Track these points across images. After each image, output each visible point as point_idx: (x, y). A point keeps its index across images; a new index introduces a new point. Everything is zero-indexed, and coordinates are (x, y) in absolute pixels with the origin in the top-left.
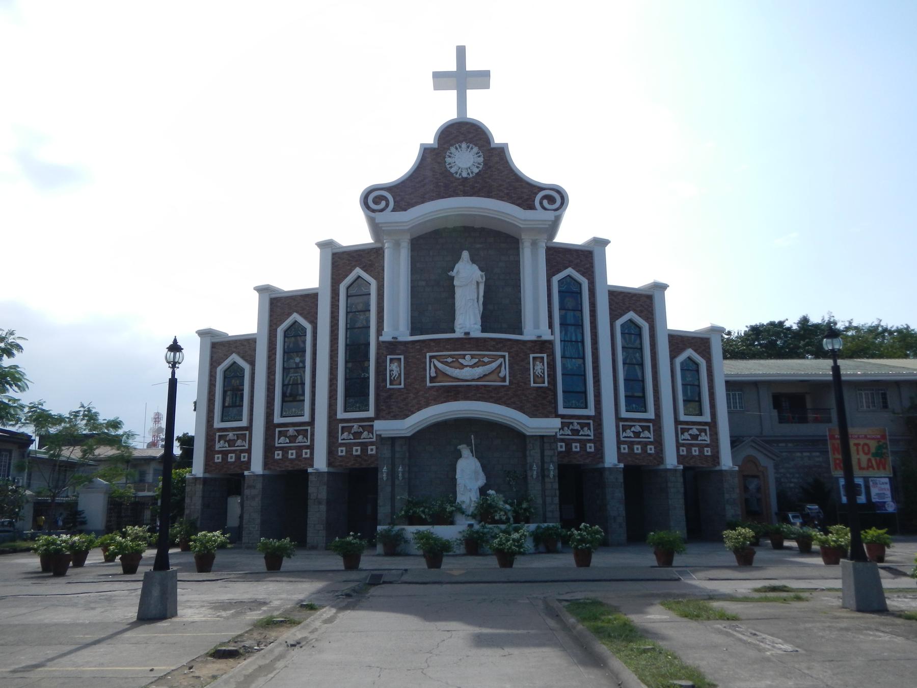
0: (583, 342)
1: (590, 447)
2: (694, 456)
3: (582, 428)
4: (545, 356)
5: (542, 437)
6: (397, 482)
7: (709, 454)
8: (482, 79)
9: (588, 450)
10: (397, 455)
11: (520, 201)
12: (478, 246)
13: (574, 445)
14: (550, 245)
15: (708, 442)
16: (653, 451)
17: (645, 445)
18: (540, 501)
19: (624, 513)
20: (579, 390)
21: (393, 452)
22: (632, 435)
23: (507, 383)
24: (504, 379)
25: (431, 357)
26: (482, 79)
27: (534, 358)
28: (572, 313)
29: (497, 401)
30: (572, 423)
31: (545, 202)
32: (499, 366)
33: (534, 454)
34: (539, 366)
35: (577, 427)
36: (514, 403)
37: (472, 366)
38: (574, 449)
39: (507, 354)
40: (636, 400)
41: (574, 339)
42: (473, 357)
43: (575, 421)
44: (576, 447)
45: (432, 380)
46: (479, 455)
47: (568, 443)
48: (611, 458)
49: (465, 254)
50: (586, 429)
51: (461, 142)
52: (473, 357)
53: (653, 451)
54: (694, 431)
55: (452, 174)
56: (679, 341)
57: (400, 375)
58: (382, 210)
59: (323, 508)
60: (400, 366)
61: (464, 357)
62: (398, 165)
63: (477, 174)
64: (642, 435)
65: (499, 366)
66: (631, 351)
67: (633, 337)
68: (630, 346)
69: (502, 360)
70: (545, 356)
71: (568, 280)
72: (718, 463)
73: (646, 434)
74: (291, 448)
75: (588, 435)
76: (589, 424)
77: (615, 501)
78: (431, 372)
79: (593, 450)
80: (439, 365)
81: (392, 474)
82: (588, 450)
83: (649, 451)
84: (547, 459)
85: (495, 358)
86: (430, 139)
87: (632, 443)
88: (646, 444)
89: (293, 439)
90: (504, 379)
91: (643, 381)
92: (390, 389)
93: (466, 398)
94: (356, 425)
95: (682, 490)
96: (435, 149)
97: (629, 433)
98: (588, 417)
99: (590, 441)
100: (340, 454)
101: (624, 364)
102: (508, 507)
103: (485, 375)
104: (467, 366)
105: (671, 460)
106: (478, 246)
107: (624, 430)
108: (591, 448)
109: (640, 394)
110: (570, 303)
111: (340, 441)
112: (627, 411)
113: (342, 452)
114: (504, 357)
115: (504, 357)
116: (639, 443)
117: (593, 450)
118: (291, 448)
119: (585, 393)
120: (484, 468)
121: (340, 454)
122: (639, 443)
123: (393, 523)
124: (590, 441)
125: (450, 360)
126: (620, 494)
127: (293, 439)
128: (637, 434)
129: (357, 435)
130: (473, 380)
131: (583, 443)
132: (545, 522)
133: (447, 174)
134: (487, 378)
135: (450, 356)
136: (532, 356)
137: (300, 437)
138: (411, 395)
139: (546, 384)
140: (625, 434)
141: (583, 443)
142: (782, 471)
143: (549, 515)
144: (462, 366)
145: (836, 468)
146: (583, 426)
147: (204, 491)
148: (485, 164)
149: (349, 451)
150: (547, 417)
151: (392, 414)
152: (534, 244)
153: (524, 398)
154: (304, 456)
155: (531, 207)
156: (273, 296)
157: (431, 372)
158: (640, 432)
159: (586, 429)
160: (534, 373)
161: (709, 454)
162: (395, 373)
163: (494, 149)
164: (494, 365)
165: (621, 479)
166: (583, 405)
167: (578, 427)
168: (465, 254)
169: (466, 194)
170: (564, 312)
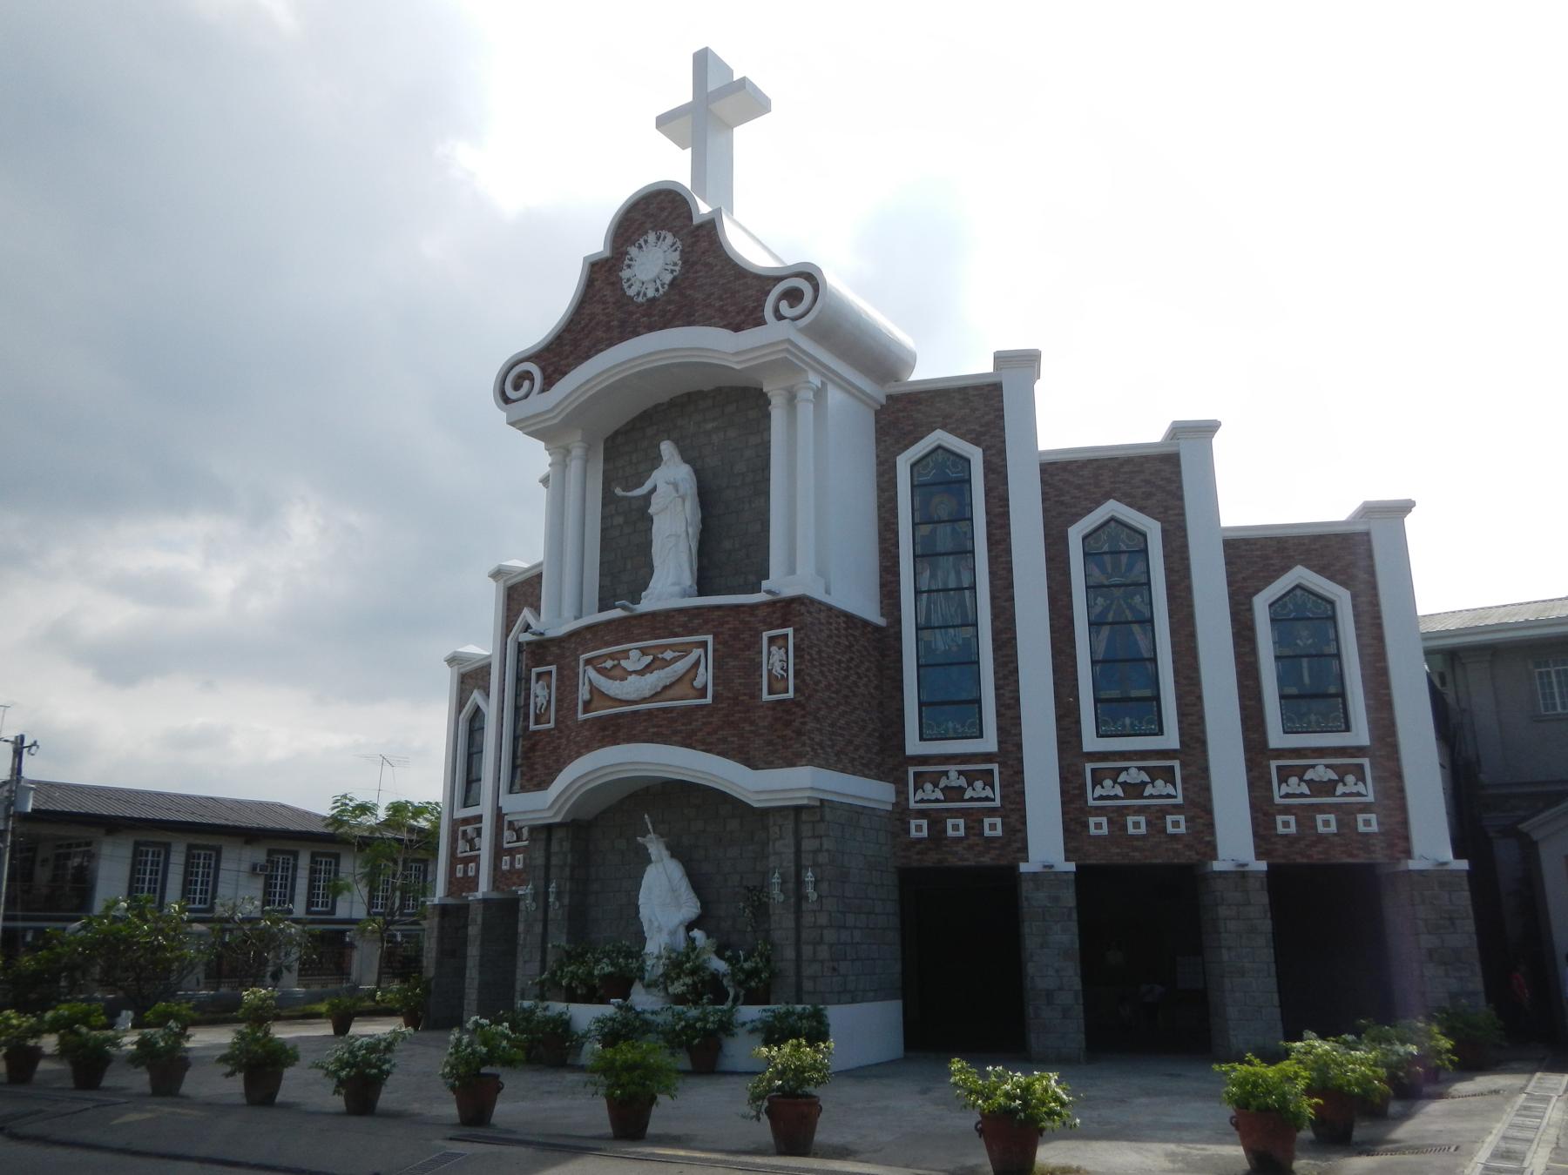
0: (973, 588)
1: (993, 827)
2: (1322, 838)
3: (970, 784)
4: (790, 631)
5: (798, 810)
6: (551, 915)
7: (1374, 828)
9: (987, 832)
10: (554, 861)
11: (738, 319)
12: (709, 426)
13: (950, 822)
14: (895, 389)
15: (1371, 798)
16: (1182, 829)
17: (1156, 816)
18: (790, 953)
19: (1077, 984)
20: (964, 696)
21: (548, 858)
22: (1119, 791)
23: (709, 700)
24: (702, 693)
25: (588, 662)
27: (772, 640)
28: (948, 528)
29: (688, 742)
30: (946, 773)
31: (784, 306)
33: (783, 847)
34: (777, 653)
35: (955, 780)
36: (724, 740)
37: (641, 673)
38: (950, 832)
39: (709, 638)
40: (1128, 703)
41: (952, 585)
42: (644, 651)
43: (953, 769)
44: (955, 828)
45: (587, 706)
46: (675, 852)
47: (937, 821)
48: (1046, 847)
49: (667, 448)
50: (979, 784)
51: (646, 233)
52: (644, 651)
53: (1182, 829)
54: (1321, 773)
55: (631, 298)
56: (1256, 556)
57: (549, 702)
58: (526, 396)
60: (549, 687)
62: (545, 308)
63: (672, 284)
64: (1149, 790)
65: (695, 665)
66: (1117, 592)
67: (1124, 558)
68: (1116, 580)
69: (701, 651)
70: (790, 631)
71: (940, 455)
72: (1408, 853)
73: (1161, 787)
75: (987, 799)
76: (991, 772)
77: (1052, 957)
78: (584, 693)
79: (999, 832)
80: (592, 673)
81: (542, 895)
82: (987, 832)
83: (1170, 830)
84: (805, 862)
85: (685, 650)
86: (596, 243)
87: (1123, 811)
88: (1163, 811)
90: (702, 693)
91: (1154, 660)
92: (535, 732)
95: (1267, 925)
96: (607, 260)
97: (1108, 787)
98: (987, 757)
99: (992, 812)
101: (1094, 625)
102: (719, 965)
103: (665, 688)
104: (631, 673)
105: (1235, 844)
106: (709, 426)
107: (1097, 781)
108: (993, 828)
109: (1147, 693)
110: (943, 506)
112: (1099, 735)
114: (704, 644)
115: (704, 644)
116: (1139, 810)
117: (999, 832)
119: (978, 701)
120: (698, 883)
122: (1139, 810)
123: (542, 998)
124: (992, 812)
125: (609, 664)
126: (1065, 935)
128: (1134, 790)
130: (644, 700)
131: (974, 819)
132: (799, 1002)
133: (624, 301)
134: (670, 693)
135: (611, 656)
136: (765, 635)
138: (564, 741)
139: (791, 694)
140: (1099, 791)
141: (974, 819)
143: (808, 985)
146: (971, 777)
147: (441, 928)
148: (685, 262)
150: (792, 764)
151: (535, 781)
152: (792, 399)
153: (748, 728)
155: (761, 322)
156: (510, 583)
157: (584, 693)
158: (1144, 784)
159: (979, 784)
160: (770, 671)
161: (1374, 828)
162: (541, 700)
163: (701, 226)
164: (681, 666)
165: (1069, 898)
166: (976, 731)
167: (963, 782)
168: (667, 448)
170: (925, 530)
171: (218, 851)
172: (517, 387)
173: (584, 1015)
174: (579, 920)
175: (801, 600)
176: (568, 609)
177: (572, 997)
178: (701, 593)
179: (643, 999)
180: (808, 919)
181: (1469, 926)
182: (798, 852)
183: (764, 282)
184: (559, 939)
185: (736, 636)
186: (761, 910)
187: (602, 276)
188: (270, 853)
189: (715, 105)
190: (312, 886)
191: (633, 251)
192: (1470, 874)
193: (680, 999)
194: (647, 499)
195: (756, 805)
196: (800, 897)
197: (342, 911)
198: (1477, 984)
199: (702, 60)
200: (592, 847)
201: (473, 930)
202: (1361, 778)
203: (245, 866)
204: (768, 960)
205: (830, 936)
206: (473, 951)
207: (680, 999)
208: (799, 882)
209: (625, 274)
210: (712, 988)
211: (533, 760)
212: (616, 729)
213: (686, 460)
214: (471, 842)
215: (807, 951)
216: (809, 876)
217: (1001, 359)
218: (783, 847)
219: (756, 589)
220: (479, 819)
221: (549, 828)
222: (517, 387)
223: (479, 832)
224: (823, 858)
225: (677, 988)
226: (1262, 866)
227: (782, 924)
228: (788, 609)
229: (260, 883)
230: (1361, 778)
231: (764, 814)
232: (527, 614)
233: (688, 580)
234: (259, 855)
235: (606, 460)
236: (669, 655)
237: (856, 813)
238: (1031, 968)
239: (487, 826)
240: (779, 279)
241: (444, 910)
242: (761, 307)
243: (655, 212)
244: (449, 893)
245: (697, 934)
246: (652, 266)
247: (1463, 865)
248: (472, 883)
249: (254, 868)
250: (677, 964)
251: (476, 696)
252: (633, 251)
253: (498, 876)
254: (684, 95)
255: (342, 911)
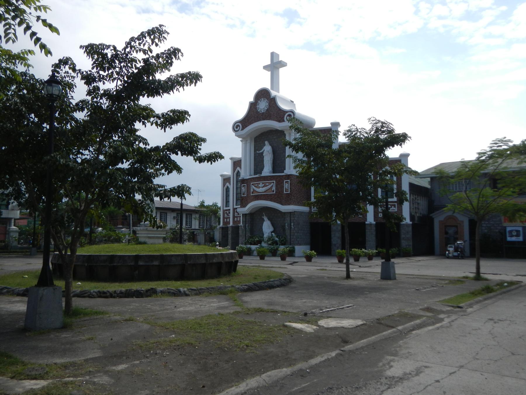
5: (290, 213)
8: (283, 64)
26: (283, 64)
31: (288, 118)
32: (272, 186)
34: (287, 185)
37: (262, 187)
42: (263, 183)
45: (253, 193)
46: (269, 219)
49: (266, 142)
61: (259, 184)
63: (267, 110)
78: (252, 190)
80: (253, 187)
84: (292, 221)
85: (270, 183)
86: (252, 99)
93: (261, 199)
95: (374, 233)
102: (277, 239)
120: (273, 224)
133: (257, 112)
142: (492, 222)
143: (292, 242)
144: (259, 187)
145: (505, 222)
148: (269, 105)
150: (289, 205)
155: (284, 121)
157: (252, 190)
164: (269, 186)
168: (266, 142)
169: (264, 119)
171: (166, 213)
172: (237, 128)
173: (253, 247)
174: (252, 231)
175: (291, 175)
176: (248, 174)
177: (251, 244)
178: (274, 172)
179: (263, 244)
180: (292, 231)
181: (411, 233)
182: (290, 220)
183: (285, 112)
184: (248, 234)
185: (279, 181)
186: (284, 230)
187: (253, 106)
188: (177, 214)
189: (275, 65)
190: (186, 222)
191: (259, 102)
192: (412, 224)
193: (270, 244)
194: (262, 153)
195: (283, 211)
196: (291, 228)
197: (193, 227)
198: (411, 243)
199: (272, 54)
200: (254, 218)
201: (230, 232)
202: (395, 207)
203: (172, 217)
204: (285, 238)
205: (296, 234)
206: (230, 236)
207: (270, 244)
208: (291, 225)
209: (258, 106)
210: (276, 243)
211: (242, 201)
212: (258, 197)
213: (270, 145)
214: (228, 214)
215: (292, 237)
216: (292, 224)
217: (332, 124)
218: (288, 219)
219: (283, 172)
220: (229, 210)
221: (246, 214)
222: (237, 128)
223: (229, 213)
224: (295, 221)
225: (270, 243)
226: (375, 223)
227: (288, 232)
228: (289, 177)
229: (175, 220)
230: (395, 207)
231: (285, 213)
232: (238, 168)
233: (271, 169)
234: (175, 214)
235: (255, 142)
236: (267, 184)
237: (301, 213)
238: (332, 240)
239: (231, 211)
240: (287, 112)
241: (222, 228)
242: (284, 117)
243: (263, 94)
244: (223, 224)
245: (273, 234)
246: (263, 106)
247: (411, 223)
248: (229, 223)
249: (174, 217)
250: (269, 239)
251: (228, 184)
252: (259, 102)
253: (234, 222)
254: (269, 63)
255: (193, 227)
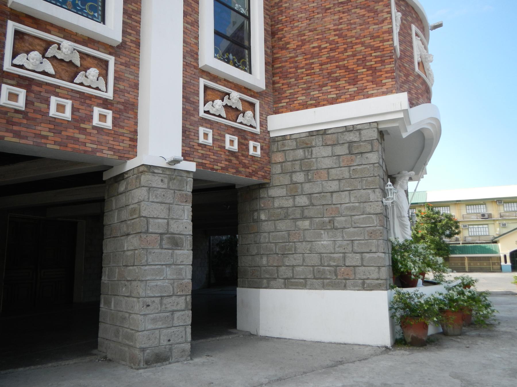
59: (186, 255)
74: (55, 91)
89: (69, 69)
94: (235, 95)
100: (202, 140)
111: (202, 114)
113: (205, 136)
118: (55, 91)
121: (202, 140)
127: (69, 69)
129: (232, 112)
137: (93, 72)
149: (219, 139)
154: (96, 121)
